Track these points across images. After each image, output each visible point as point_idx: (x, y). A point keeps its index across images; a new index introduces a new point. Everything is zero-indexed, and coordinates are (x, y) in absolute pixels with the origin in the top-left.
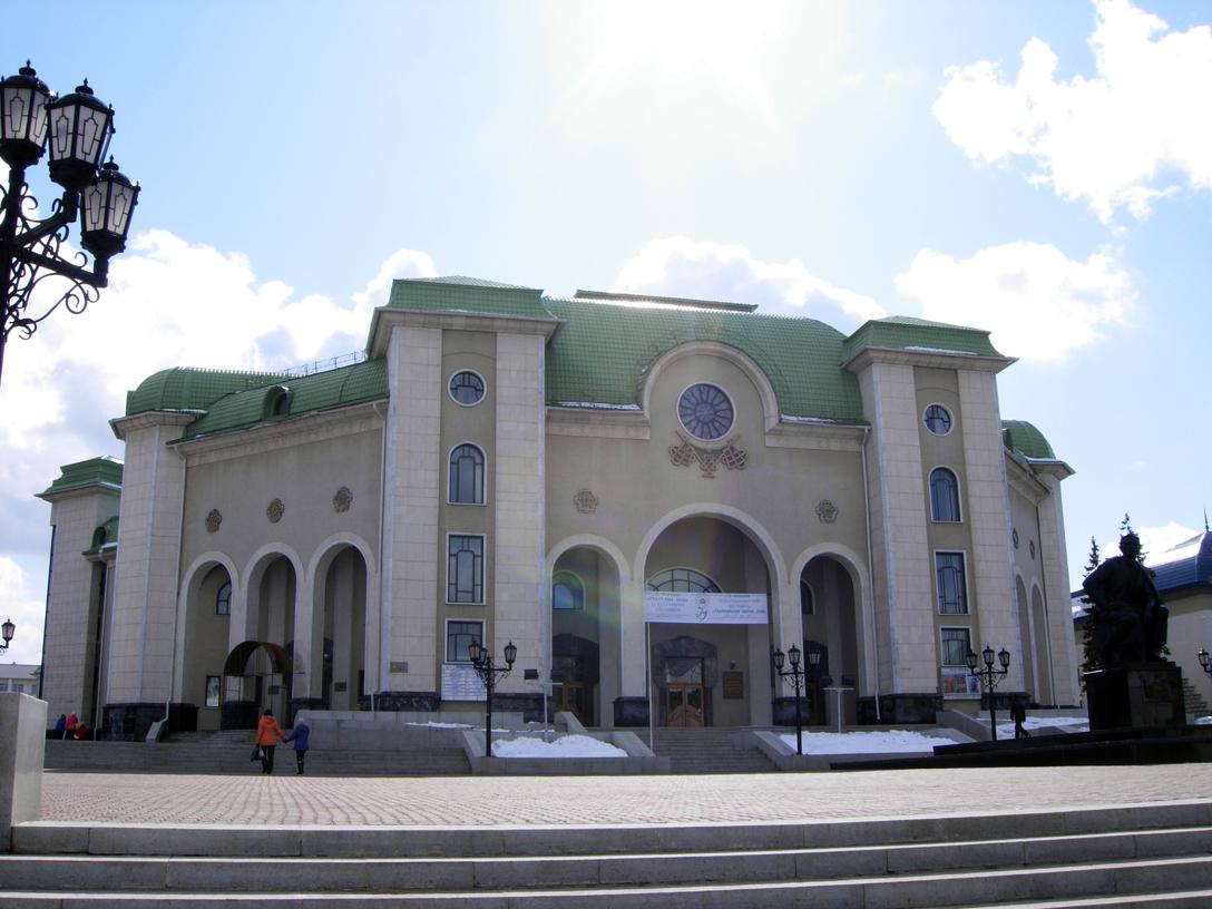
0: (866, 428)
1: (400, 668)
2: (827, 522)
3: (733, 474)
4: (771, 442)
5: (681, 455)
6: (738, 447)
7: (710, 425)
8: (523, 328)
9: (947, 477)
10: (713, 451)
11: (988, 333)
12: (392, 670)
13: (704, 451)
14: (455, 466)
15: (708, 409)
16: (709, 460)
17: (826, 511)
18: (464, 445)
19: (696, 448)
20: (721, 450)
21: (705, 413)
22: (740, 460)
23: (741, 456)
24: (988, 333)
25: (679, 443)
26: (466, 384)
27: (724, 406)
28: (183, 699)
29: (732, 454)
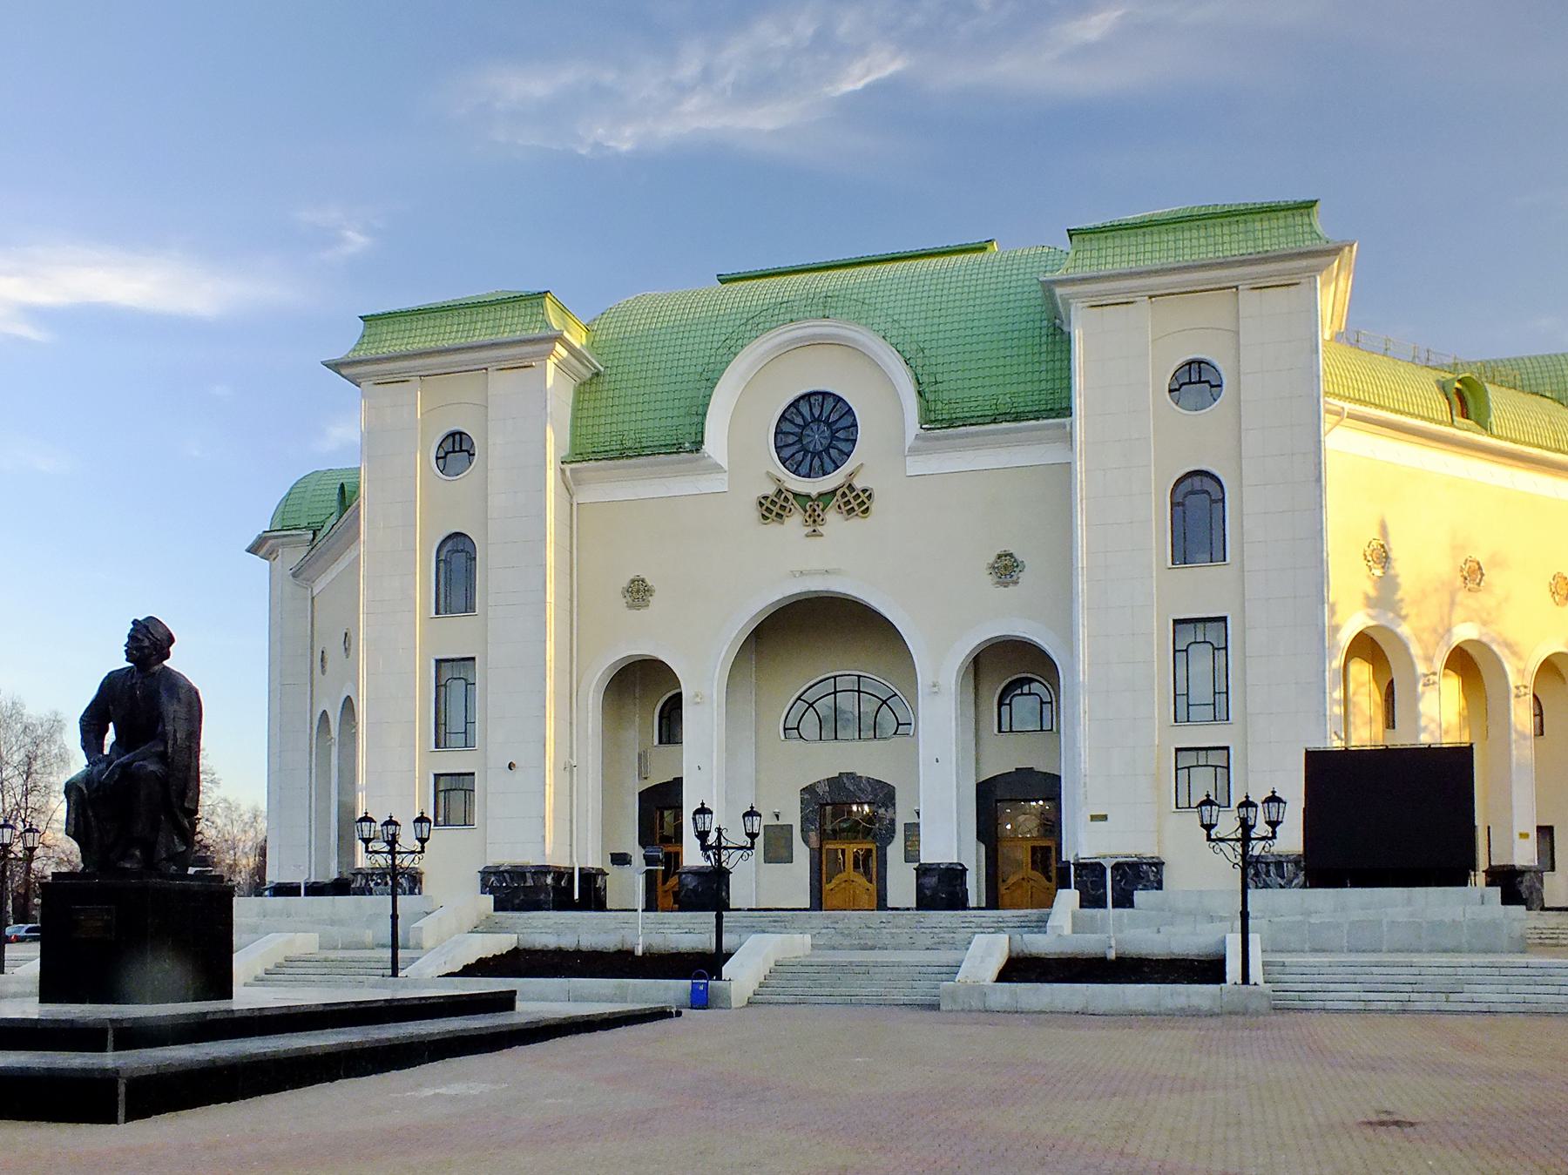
3: (856, 523)
4: (915, 466)
5: (773, 507)
6: (859, 484)
9: (1209, 485)
10: (820, 495)
13: (808, 496)
15: (816, 432)
16: (814, 508)
17: (1006, 568)
18: (449, 537)
19: (796, 495)
20: (834, 492)
22: (863, 503)
23: (863, 497)
25: (770, 490)
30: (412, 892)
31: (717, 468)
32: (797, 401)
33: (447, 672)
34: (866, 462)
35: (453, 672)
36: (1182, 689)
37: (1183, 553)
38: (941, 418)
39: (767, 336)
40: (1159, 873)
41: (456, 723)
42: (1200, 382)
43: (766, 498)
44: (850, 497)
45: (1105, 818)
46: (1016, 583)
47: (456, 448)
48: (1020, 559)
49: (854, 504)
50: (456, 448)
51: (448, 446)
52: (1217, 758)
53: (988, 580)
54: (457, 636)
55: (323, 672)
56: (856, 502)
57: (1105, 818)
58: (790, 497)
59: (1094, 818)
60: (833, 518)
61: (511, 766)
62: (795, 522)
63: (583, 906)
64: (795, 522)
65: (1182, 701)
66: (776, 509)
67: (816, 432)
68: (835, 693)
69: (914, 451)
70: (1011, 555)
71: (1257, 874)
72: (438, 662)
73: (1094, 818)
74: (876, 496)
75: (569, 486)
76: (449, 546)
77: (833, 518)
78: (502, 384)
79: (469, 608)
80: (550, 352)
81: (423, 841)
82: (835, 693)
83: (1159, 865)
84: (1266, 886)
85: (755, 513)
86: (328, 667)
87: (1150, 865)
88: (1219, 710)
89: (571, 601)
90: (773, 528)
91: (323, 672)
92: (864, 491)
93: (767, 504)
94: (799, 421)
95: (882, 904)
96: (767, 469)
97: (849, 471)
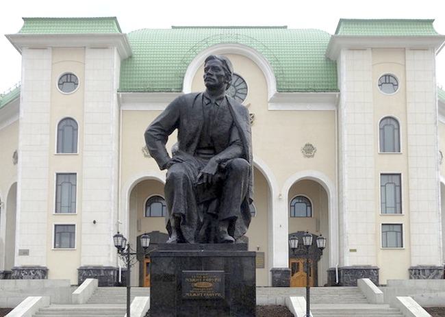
0: (337, 93)
1: (25, 253)
2: (309, 157)
4: (272, 107)
8: (100, 44)
9: (393, 122)
11: (432, 21)
12: (20, 254)
14: (61, 132)
17: (309, 150)
24: (432, 21)
26: (69, 81)
33: (62, 179)
35: (66, 181)
36: (384, 201)
37: (384, 149)
40: (377, 273)
41: (65, 202)
42: (389, 83)
45: (355, 250)
48: (314, 147)
50: (68, 81)
51: (64, 79)
52: (397, 228)
54: (66, 164)
57: (355, 250)
59: (351, 250)
61: (94, 222)
65: (384, 205)
69: (272, 101)
70: (311, 145)
71: (415, 274)
72: (57, 174)
73: (351, 250)
74: (256, 116)
76: (64, 123)
79: (73, 150)
83: (377, 270)
84: (419, 278)
87: (374, 270)
88: (398, 209)
89: (119, 152)
92: (251, 115)
94: (237, 84)
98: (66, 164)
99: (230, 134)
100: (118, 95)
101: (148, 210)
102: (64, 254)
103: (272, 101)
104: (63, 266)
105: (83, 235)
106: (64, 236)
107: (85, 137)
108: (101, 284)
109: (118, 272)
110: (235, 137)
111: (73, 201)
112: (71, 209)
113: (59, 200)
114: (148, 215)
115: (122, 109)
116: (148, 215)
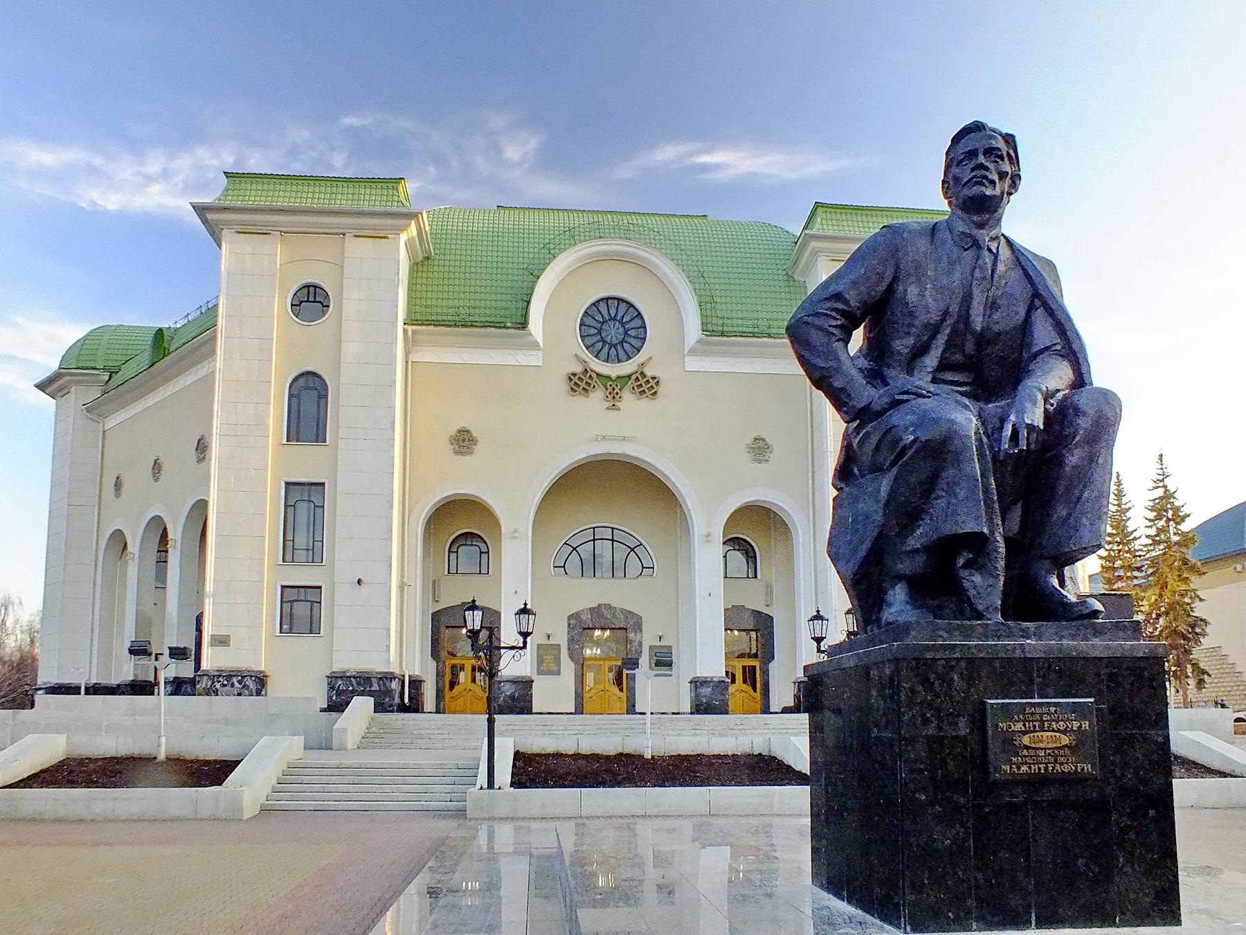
4: (692, 364)
5: (580, 383)
6: (649, 372)
7: (619, 347)
10: (618, 377)
13: (608, 377)
14: (295, 400)
15: (613, 326)
16: (614, 388)
18: (302, 375)
19: (598, 375)
20: (629, 376)
21: (613, 332)
23: (652, 383)
25: (578, 369)
26: (311, 299)
27: (623, 307)
28: (135, 675)
29: (642, 381)
30: (258, 693)
31: (535, 345)
32: (602, 300)
33: (295, 495)
34: (653, 355)
35: (304, 497)
38: (716, 330)
39: (580, 246)
41: (302, 540)
43: (575, 375)
44: (642, 381)
46: (767, 461)
47: (311, 300)
49: (645, 387)
50: (311, 300)
53: (746, 457)
55: (118, 495)
56: (646, 386)
58: (594, 376)
60: (628, 398)
61: (359, 582)
62: (597, 397)
63: (403, 709)
64: (597, 397)
66: (583, 385)
67: (613, 326)
68: (594, 540)
69: (692, 352)
70: (763, 440)
74: (662, 382)
75: (411, 344)
76: (302, 381)
77: (628, 398)
78: (358, 250)
79: (319, 436)
80: (405, 228)
81: (525, 635)
82: (594, 540)
85: (564, 387)
86: (124, 490)
90: (579, 400)
91: (118, 495)
92: (653, 378)
93: (575, 379)
95: (631, 709)
96: (573, 352)
97: (641, 361)
98: (307, 462)
99: (1026, 327)
100: (405, 331)
101: (453, 556)
102: (301, 644)
103: (692, 352)
104: (299, 673)
105: (340, 609)
106: (300, 610)
107: (344, 411)
108: (380, 708)
109: (403, 682)
110: (1043, 333)
111: (318, 538)
112: (314, 554)
113: (289, 537)
114: (453, 570)
115: (412, 358)
116: (453, 570)
